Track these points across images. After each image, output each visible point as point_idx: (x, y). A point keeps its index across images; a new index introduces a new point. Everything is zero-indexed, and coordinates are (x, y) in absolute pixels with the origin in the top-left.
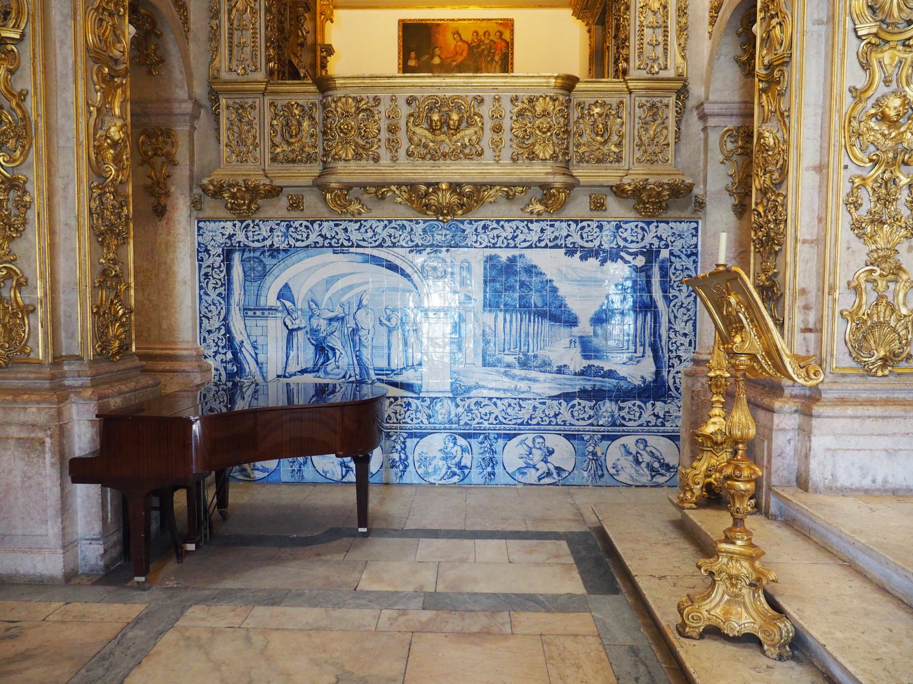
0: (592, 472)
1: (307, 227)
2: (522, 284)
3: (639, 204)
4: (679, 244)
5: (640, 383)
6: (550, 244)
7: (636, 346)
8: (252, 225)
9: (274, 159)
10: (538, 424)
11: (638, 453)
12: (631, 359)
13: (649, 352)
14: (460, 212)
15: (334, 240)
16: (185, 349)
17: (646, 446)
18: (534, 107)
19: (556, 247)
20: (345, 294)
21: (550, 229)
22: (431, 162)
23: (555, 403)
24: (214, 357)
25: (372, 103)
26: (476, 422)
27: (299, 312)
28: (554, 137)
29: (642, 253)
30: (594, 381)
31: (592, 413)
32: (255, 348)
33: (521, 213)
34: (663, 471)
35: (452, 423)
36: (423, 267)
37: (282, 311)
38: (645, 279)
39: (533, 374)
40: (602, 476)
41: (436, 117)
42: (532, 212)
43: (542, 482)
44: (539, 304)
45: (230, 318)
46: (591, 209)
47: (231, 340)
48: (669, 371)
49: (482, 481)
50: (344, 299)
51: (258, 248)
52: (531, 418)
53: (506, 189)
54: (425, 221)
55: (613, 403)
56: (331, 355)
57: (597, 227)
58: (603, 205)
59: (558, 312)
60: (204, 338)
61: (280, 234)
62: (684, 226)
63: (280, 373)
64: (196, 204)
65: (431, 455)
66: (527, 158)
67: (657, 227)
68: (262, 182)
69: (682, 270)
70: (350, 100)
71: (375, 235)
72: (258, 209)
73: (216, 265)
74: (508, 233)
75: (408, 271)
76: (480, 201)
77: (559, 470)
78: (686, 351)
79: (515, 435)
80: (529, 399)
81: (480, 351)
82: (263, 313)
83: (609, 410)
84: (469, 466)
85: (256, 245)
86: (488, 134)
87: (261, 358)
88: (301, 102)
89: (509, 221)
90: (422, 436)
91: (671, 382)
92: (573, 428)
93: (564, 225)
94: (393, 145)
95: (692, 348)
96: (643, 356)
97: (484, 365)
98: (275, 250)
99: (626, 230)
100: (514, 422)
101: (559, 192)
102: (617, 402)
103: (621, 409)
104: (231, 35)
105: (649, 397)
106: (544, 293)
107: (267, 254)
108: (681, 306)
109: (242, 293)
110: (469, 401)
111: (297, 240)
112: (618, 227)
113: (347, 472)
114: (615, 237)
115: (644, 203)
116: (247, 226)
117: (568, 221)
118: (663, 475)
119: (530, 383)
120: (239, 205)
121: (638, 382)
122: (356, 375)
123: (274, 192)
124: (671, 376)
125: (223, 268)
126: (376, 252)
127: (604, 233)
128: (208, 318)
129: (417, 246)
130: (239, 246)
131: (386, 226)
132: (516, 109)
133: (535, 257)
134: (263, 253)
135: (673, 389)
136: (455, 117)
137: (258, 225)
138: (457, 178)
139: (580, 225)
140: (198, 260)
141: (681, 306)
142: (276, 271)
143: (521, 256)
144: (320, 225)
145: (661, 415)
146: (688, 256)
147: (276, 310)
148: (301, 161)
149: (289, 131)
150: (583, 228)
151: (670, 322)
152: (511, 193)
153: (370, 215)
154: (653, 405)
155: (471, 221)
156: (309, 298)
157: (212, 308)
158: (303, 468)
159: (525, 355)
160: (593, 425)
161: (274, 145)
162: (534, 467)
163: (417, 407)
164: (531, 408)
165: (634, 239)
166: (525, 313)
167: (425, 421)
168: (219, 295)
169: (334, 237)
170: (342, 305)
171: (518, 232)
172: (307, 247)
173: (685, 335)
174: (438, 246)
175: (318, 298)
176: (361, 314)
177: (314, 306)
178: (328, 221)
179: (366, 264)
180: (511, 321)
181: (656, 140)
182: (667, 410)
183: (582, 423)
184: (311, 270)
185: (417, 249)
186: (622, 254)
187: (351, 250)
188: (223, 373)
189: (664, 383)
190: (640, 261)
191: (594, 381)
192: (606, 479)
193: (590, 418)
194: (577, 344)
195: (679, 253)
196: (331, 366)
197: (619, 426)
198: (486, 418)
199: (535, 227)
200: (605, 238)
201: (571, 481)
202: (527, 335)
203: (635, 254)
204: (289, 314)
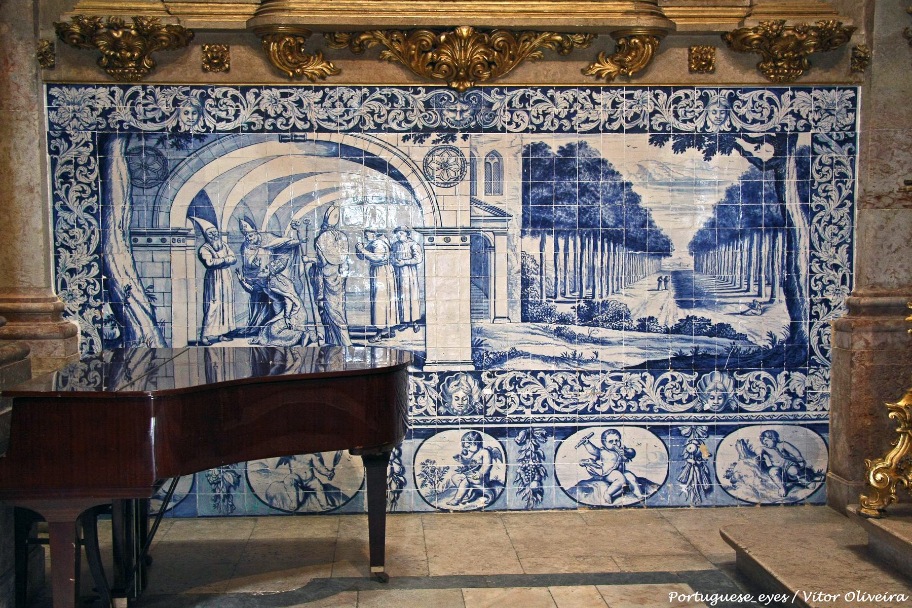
0: (694, 484)
1: (235, 98)
2: (584, 190)
3: (765, 61)
4: (826, 124)
5: (767, 343)
6: (627, 126)
7: (760, 286)
8: (142, 94)
10: (610, 411)
11: (764, 452)
12: (752, 306)
13: (781, 296)
14: (486, 75)
15: (280, 120)
16: (33, 301)
17: (777, 441)
19: (637, 130)
20: (301, 207)
21: (626, 103)
23: (636, 377)
24: (81, 313)
26: (512, 410)
27: (225, 238)
29: (770, 140)
30: (696, 341)
31: (692, 391)
32: (151, 298)
33: (580, 76)
34: (804, 481)
35: (475, 413)
36: (426, 163)
37: (195, 237)
38: (773, 180)
39: (601, 333)
40: (710, 490)
42: (598, 75)
43: (617, 502)
44: (610, 221)
45: (107, 249)
46: (691, 71)
47: (109, 284)
48: (811, 325)
49: (524, 503)
50: (297, 216)
51: (154, 133)
52: (599, 403)
53: (559, 38)
54: (428, 90)
55: (726, 376)
56: (277, 308)
57: (700, 98)
58: (709, 63)
59: (640, 235)
60: (64, 281)
61: (190, 109)
62: (834, 95)
63: (193, 338)
64: (44, 58)
65: (439, 464)
67: (793, 97)
68: (164, 23)
69: (831, 166)
71: (347, 112)
72: (153, 69)
73: (82, 160)
74: (560, 107)
75: (404, 170)
76: (519, 59)
77: (643, 483)
78: (837, 292)
79: (574, 430)
80: (597, 373)
81: (517, 295)
82: (163, 241)
83: (720, 386)
84: (502, 480)
85: (150, 127)
87: (161, 314)
89: (562, 89)
90: (428, 434)
91: (814, 340)
92: (664, 415)
93: (649, 95)
95: (847, 288)
96: (771, 301)
97: (524, 319)
98: (182, 136)
99: (745, 103)
100: (572, 408)
101: (644, 43)
102: (731, 375)
103: (737, 384)
105: (780, 366)
106: (618, 204)
107: (169, 142)
108: (830, 222)
109: (127, 208)
110: (500, 377)
111: (220, 120)
112: (732, 99)
113: (306, 496)
114: (728, 114)
115: (776, 60)
116: (135, 95)
117: (655, 88)
118: (803, 486)
119: (598, 348)
120: (124, 61)
121: (763, 342)
122: (319, 338)
124: (814, 331)
125: (94, 165)
126: (349, 140)
127: (711, 108)
128: (68, 248)
129: (416, 129)
130: (121, 129)
131: (365, 97)
133: (604, 147)
134: (162, 140)
135: (817, 351)
137: (152, 94)
138: (485, 20)
139: (673, 96)
140: (51, 152)
141: (830, 222)
142: (184, 171)
143: (582, 145)
144: (257, 95)
145: (800, 392)
146: (841, 143)
147: (185, 234)
150: (677, 100)
151: (812, 247)
152: (567, 45)
153: (338, 78)
154: (787, 377)
155: (502, 88)
156: (241, 211)
157: (77, 231)
158: (233, 492)
159: (588, 303)
160: (693, 410)
162: (604, 479)
163: (418, 388)
164: (598, 386)
165: (758, 117)
166: (588, 235)
167: (433, 412)
168: (89, 210)
169: (281, 115)
170: (295, 226)
171: (577, 107)
172: (236, 130)
173: (836, 267)
174: (449, 129)
175: (256, 214)
176: (327, 239)
177: (249, 228)
178: (270, 88)
179: (333, 160)
180: (566, 249)
182: (808, 384)
183: (678, 407)
184: (244, 169)
185: (419, 134)
186: (740, 141)
187: (310, 135)
188: (97, 340)
189: (804, 342)
190: (766, 152)
191: (696, 341)
192: (718, 495)
193: (690, 399)
194: (670, 284)
195: (827, 138)
196: (278, 325)
197: (736, 411)
198: (529, 403)
199: (603, 98)
200: (712, 117)
201: (661, 500)
202: (592, 270)
203: (758, 141)
204: (207, 241)
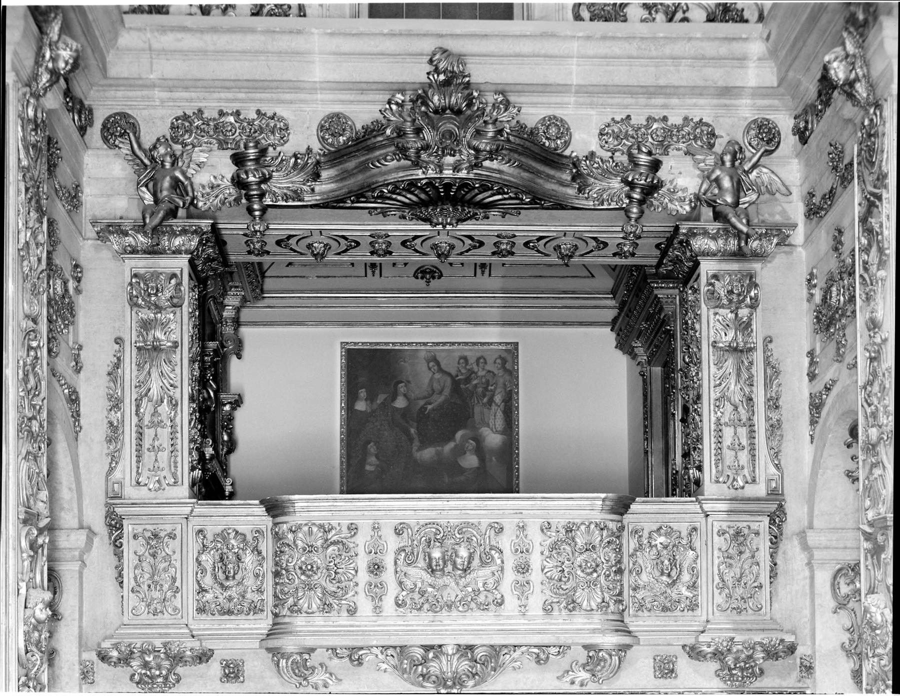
9: (201, 610)
14: (471, 683)
18: (573, 539)
22: (430, 614)
25: (345, 533)
28: (602, 578)
41: (436, 554)
58: (672, 671)
66: (566, 608)
70: (315, 529)
86: (510, 576)
88: (240, 529)
94: (376, 593)
101: (611, 656)
104: (140, 435)
115: (730, 669)
123: (204, 657)
132: (549, 541)
136: (463, 553)
148: (240, 612)
149: (227, 569)
161: (202, 590)
181: (744, 580)
